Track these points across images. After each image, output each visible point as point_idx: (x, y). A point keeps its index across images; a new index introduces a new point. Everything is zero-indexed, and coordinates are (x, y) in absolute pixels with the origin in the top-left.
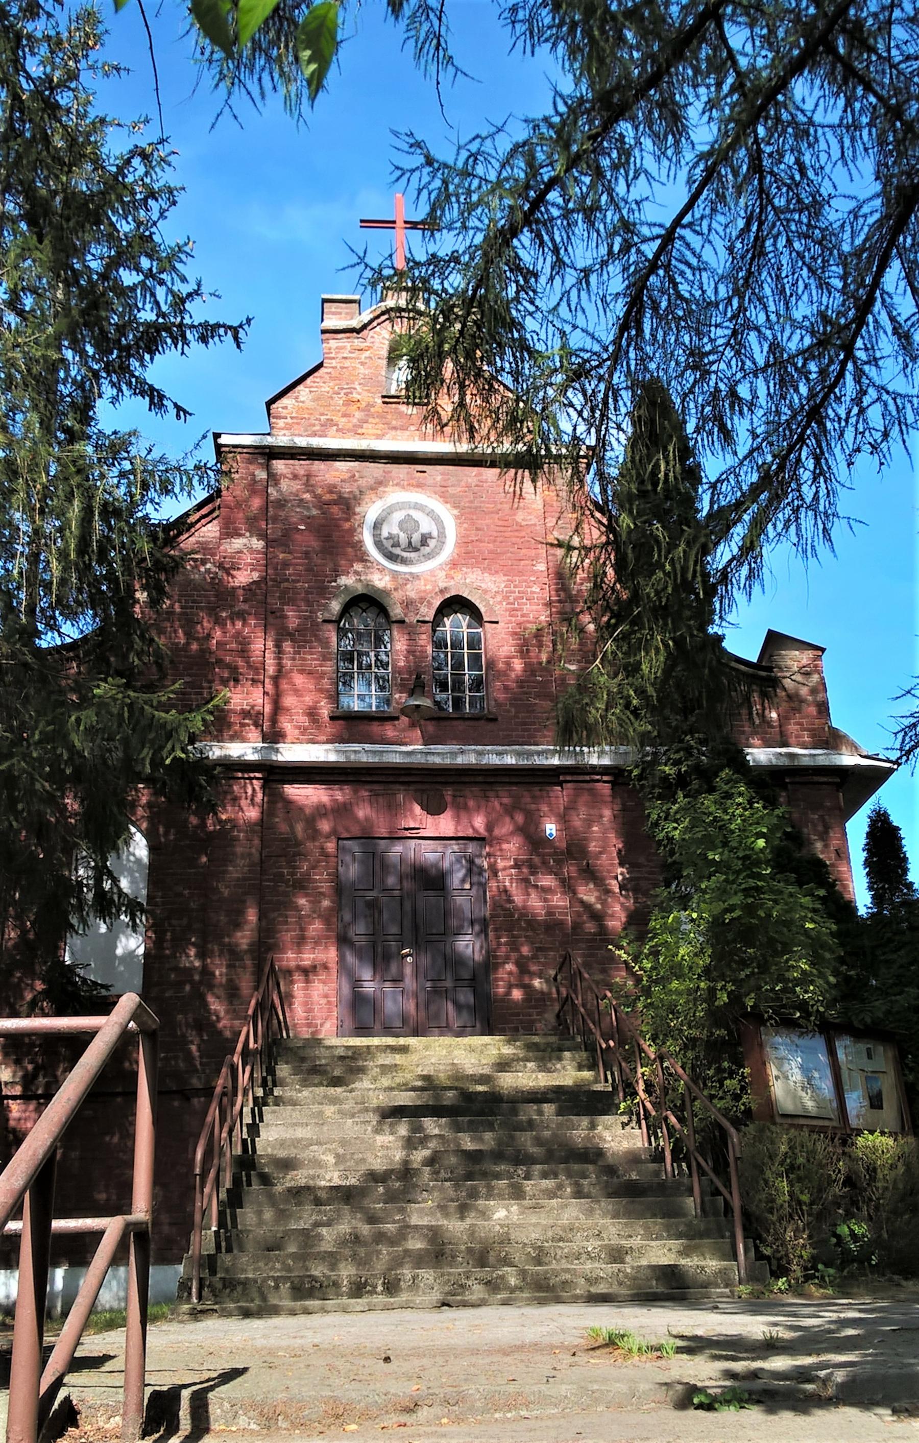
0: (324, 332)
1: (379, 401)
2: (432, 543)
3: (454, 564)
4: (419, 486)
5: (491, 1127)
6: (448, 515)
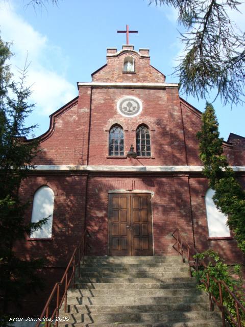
0: (107, 57)
1: (122, 73)
2: (136, 109)
3: (142, 115)
4: (132, 94)
5: (68, 195)
6: (140, 102)
